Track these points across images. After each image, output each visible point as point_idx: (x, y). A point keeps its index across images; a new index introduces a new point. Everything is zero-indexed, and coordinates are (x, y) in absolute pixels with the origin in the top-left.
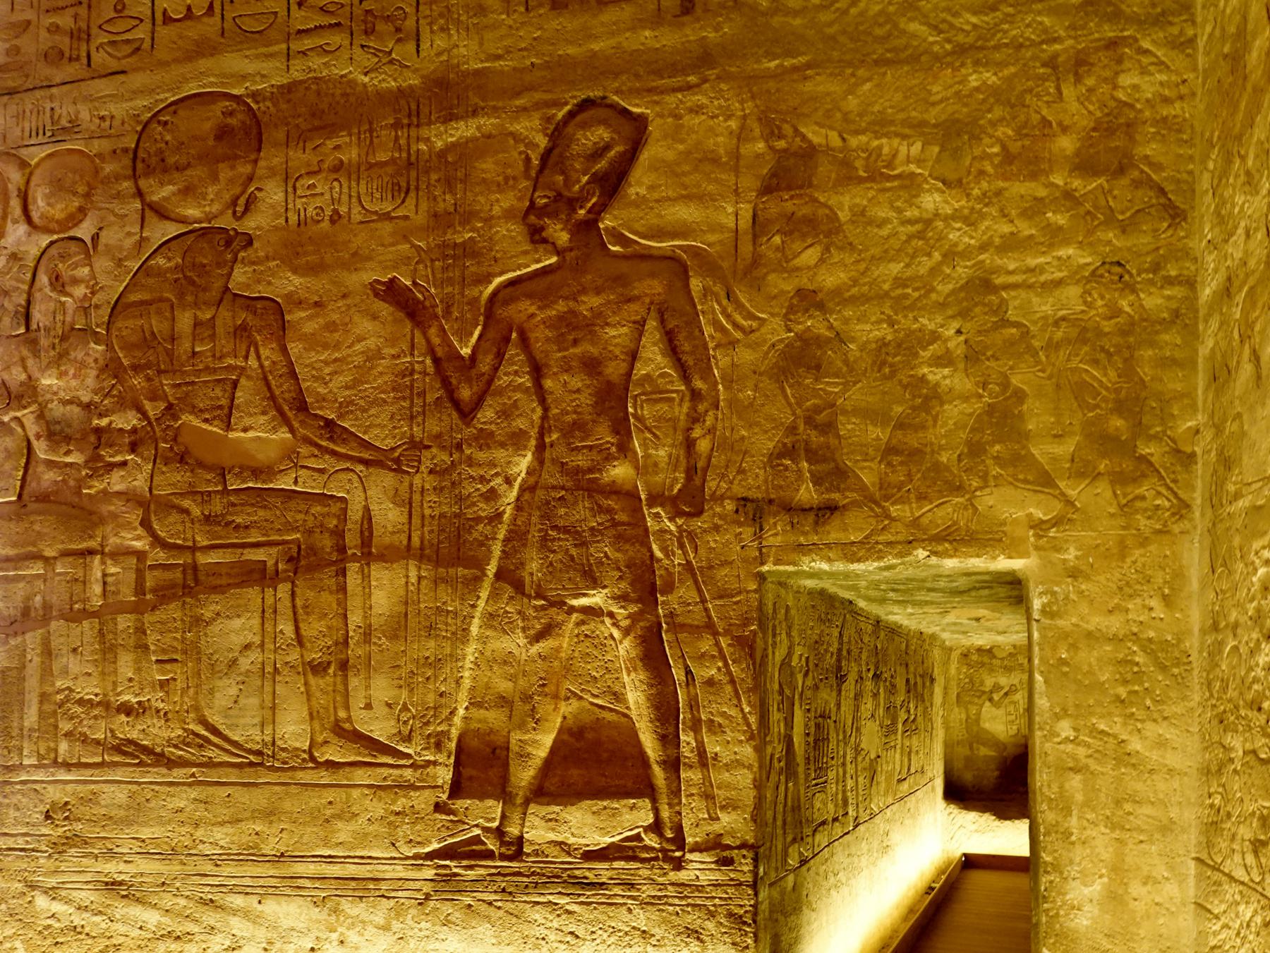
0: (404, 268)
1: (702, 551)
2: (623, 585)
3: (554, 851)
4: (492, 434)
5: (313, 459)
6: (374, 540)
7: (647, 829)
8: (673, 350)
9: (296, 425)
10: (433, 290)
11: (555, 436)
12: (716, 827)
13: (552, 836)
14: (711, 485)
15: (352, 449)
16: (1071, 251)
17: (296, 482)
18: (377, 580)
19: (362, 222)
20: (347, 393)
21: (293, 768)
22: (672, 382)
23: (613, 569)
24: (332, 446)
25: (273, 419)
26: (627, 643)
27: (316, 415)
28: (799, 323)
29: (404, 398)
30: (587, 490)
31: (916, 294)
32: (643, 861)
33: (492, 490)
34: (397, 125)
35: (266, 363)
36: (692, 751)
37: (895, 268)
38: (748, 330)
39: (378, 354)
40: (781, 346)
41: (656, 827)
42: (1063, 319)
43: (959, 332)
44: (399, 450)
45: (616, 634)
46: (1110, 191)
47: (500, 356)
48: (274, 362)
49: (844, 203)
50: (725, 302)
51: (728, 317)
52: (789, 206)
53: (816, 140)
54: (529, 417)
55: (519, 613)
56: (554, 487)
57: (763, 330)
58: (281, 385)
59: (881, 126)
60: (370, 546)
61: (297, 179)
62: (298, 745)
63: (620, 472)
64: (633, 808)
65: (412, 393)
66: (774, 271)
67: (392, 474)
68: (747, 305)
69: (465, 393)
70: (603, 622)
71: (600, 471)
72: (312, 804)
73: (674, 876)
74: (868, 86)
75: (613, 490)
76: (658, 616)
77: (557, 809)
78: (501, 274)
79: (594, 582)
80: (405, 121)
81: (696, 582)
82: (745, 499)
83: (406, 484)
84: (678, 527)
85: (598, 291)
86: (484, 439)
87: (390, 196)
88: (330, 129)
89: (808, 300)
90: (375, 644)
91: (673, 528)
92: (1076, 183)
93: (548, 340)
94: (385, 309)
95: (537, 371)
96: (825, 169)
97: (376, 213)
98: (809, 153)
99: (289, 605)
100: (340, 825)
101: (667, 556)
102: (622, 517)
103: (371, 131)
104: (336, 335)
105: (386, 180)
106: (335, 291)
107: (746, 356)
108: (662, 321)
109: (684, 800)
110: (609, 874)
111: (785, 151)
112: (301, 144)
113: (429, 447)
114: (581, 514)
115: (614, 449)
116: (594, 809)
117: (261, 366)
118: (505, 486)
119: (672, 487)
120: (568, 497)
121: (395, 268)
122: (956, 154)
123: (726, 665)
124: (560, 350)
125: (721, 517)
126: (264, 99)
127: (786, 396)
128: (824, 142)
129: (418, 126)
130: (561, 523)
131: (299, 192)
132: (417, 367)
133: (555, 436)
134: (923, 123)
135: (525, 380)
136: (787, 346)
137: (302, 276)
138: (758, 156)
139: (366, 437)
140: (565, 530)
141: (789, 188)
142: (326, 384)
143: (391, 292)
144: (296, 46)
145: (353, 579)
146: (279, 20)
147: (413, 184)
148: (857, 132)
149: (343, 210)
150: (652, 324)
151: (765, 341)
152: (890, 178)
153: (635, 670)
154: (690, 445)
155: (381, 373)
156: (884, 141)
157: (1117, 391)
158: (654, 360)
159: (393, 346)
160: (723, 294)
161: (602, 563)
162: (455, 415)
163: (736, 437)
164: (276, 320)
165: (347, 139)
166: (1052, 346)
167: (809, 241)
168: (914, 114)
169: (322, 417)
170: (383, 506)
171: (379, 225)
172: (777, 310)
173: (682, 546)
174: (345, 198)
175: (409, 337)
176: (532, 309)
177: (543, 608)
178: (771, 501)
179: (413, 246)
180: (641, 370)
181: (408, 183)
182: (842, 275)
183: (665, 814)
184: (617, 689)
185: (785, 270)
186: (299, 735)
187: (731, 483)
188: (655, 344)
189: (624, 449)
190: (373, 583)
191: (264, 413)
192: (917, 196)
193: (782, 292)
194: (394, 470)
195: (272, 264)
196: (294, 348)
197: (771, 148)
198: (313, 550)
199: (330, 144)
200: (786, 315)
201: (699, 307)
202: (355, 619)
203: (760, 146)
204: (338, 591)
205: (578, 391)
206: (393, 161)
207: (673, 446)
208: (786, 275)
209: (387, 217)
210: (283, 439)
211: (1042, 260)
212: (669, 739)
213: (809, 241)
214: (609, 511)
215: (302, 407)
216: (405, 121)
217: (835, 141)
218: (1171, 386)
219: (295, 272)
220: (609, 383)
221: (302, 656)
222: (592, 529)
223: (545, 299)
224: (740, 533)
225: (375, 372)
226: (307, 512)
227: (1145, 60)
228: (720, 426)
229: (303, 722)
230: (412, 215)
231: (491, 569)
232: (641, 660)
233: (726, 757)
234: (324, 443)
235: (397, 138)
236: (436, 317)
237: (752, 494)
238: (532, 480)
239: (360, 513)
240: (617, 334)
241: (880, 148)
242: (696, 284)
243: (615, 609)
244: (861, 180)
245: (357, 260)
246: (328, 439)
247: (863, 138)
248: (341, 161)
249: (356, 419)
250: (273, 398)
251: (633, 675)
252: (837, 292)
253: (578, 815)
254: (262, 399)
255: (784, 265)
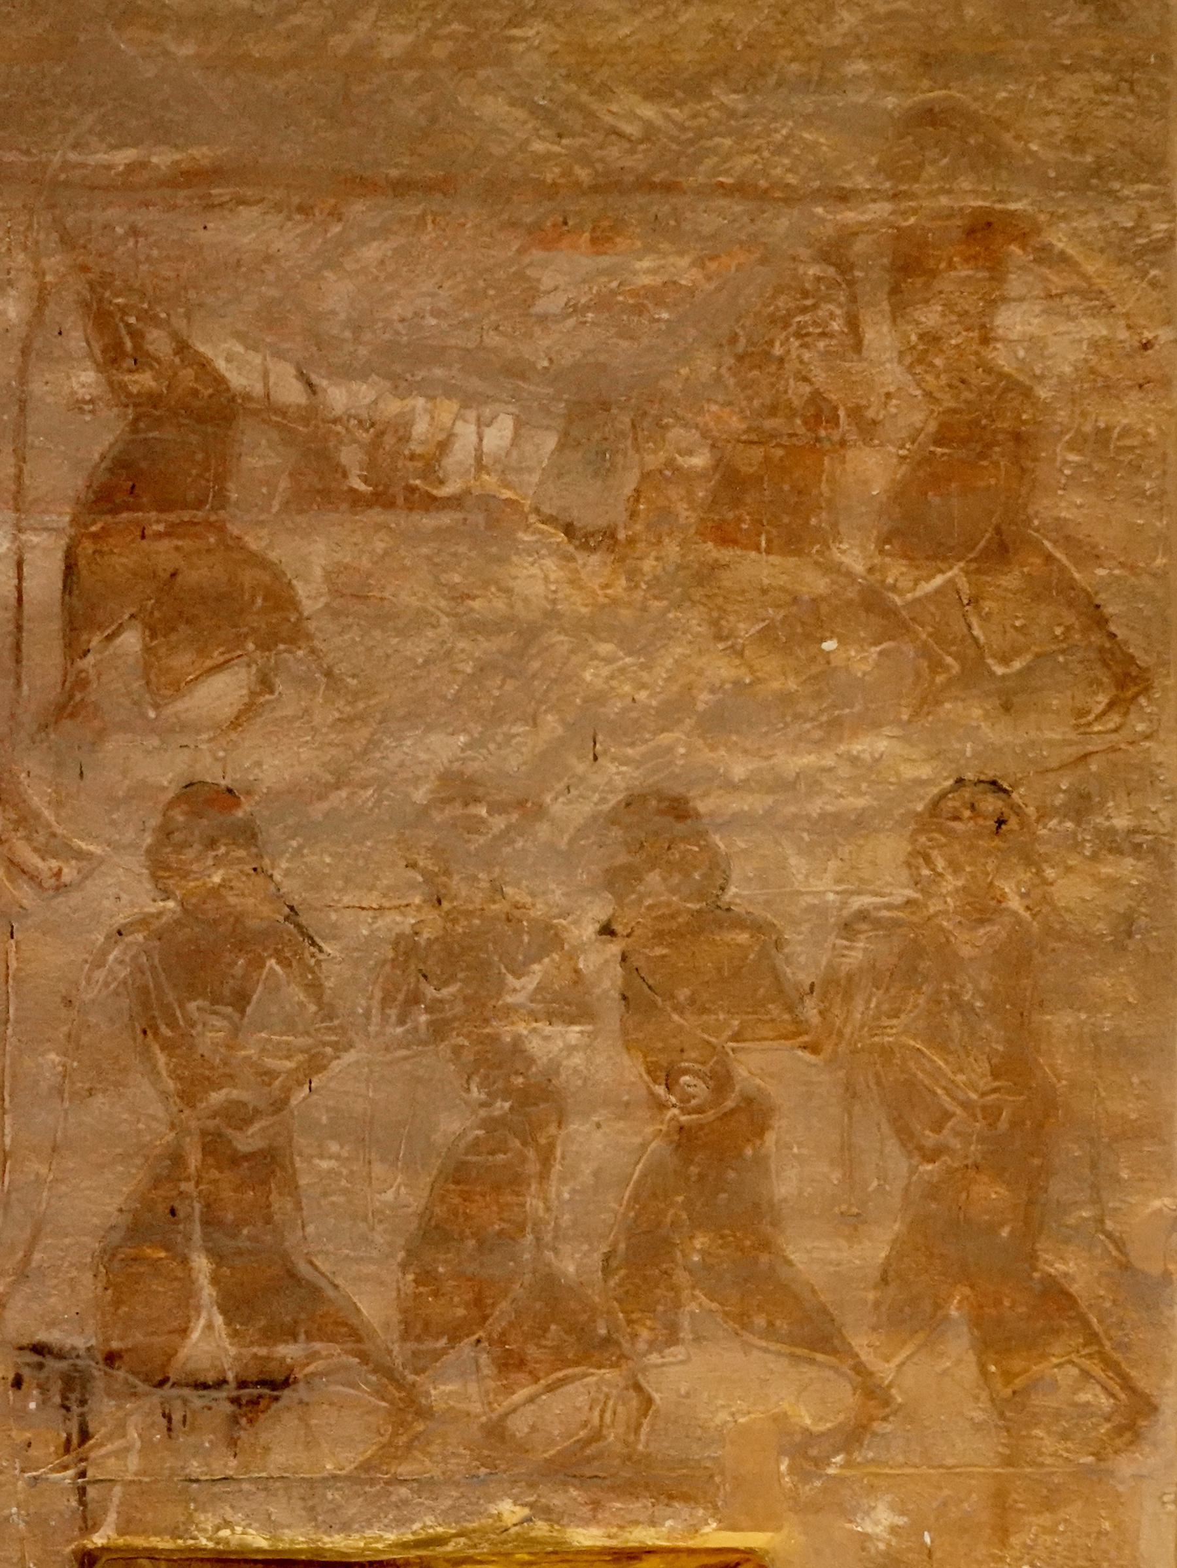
16: (882, 745)
31: (499, 823)
37: (443, 748)
42: (863, 915)
43: (607, 930)
46: (974, 601)
49: (311, 557)
53: (237, 380)
92: (896, 571)
96: (260, 457)
111: (154, 399)
122: (602, 465)
128: (258, 389)
134: (517, 370)
138: (78, 405)
148: (347, 373)
152: (432, 503)
157: (991, 1114)
166: (837, 986)
167: (217, 657)
168: (493, 340)
182: (305, 753)
192: (502, 560)
197: (117, 388)
203: (86, 379)
211: (809, 760)
213: (217, 657)
217: (291, 393)
218: (1114, 1106)
227: (1058, 281)
244: (356, 501)
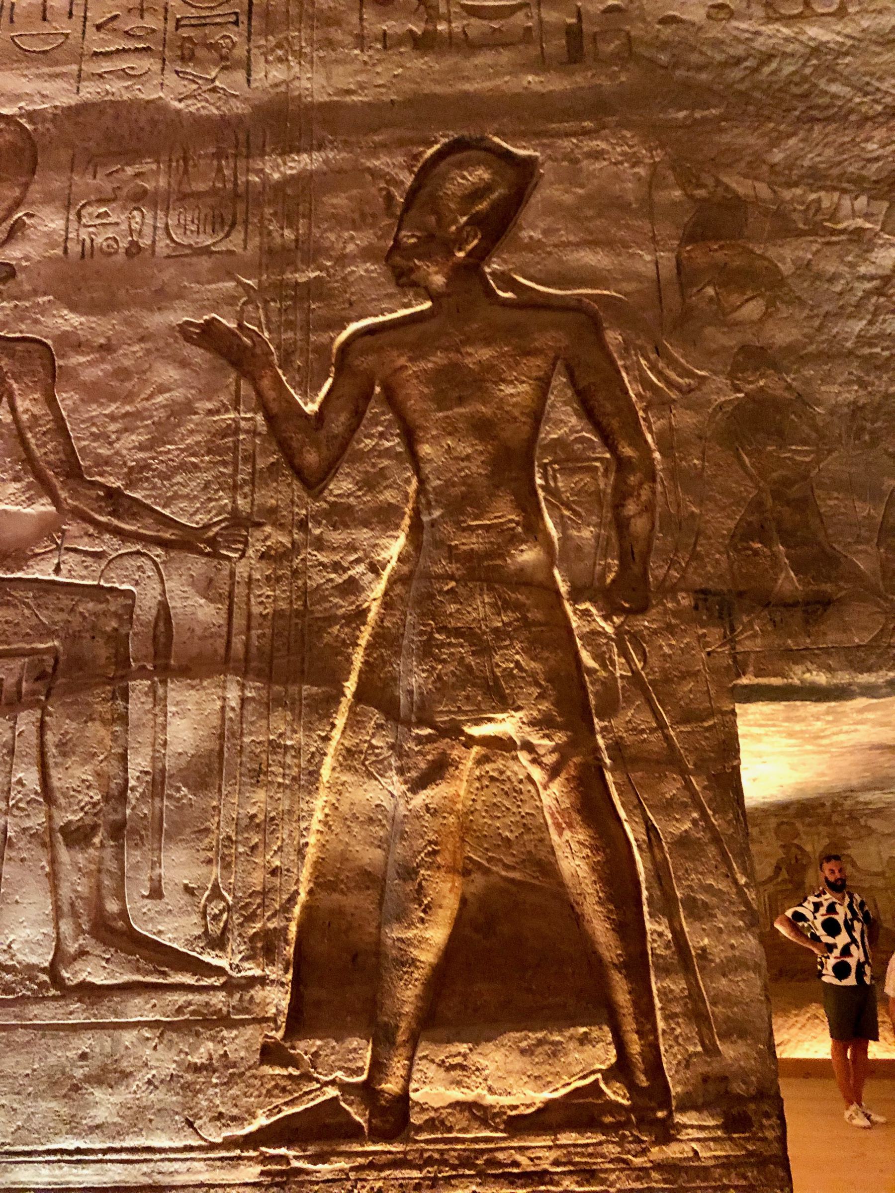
0: (227, 308)
1: (654, 661)
2: (544, 706)
3: (459, 1120)
4: (350, 507)
5: (86, 539)
6: (174, 648)
7: (609, 1075)
8: (589, 412)
9: (63, 494)
10: (266, 335)
11: (437, 513)
12: (716, 1067)
13: (457, 1094)
14: (657, 570)
15: (145, 527)
17: (57, 570)
18: (177, 704)
19: (169, 257)
20: (141, 455)
21: (22, 1000)
22: (594, 449)
23: (529, 684)
24: (116, 522)
25: (29, 487)
26: (556, 787)
27: (94, 484)
28: (750, 383)
29: (224, 464)
30: (487, 580)
32: (605, 1129)
33: (352, 580)
34: (219, 155)
35: (25, 417)
36: (667, 947)
38: (685, 389)
39: (188, 408)
40: (729, 409)
41: (621, 1070)
44: (216, 529)
45: (538, 774)
47: (358, 414)
48: (34, 416)
50: (653, 356)
51: (660, 374)
52: (720, 256)
54: (400, 490)
55: (392, 747)
56: (438, 577)
57: (705, 389)
58: (44, 445)
59: (816, 178)
60: (168, 657)
61: (84, 206)
62: (33, 960)
63: (528, 555)
64: (584, 1040)
65: (236, 458)
66: (710, 324)
67: (204, 560)
68: (682, 361)
69: (311, 458)
70: (515, 758)
71: (502, 556)
72: (52, 1060)
73: (656, 1153)
74: (792, 141)
75: (523, 580)
76: (597, 749)
77: (463, 1048)
78: (359, 318)
79: (505, 703)
80: (231, 151)
81: (649, 701)
82: (704, 592)
83: (226, 572)
84: (617, 628)
85: (488, 342)
86: (340, 515)
87: (209, 229)
88: (132, 155)
89: (755, 357)
90: (170, 797)
91: (609, 630)
93: (423, 396)
94: (197, 355)
95: (410, 437)
97: (190, 246)
98: (736, 204)
99: (34, 740)
100: (99, 1094)
101: (604, 666)
102: (535, 615)
103: (185, 160)
104: (128, 385)
105: (204, 211)
106: (129, 332)
107: (685, 419)
108: (573, 381)
109: (661, 1025)
110: (553, 1155)
112: (91, 169)
113: (259, 525)
114: (479, 610)
115: (520, 529)
116: (524, 1044)
117: (16, 420)
118: (371, 576)
119: (603, 576)
120: (461, 590)
121: (214, 309)
123: (704, 816)
124: (440, 410)
125: (675, 614)
126: (44, 120)
127: (743, 465)
128: (752, 193)
129: (247, 157)
130: (453, 623)
131: (84, 221)
132: (243, 424)
133: (437, 513)
135: (393, 443)
136: (735, 408)
137: (82, 314)
139: (167, 512)
140: (457, 632)
141: (717, 238)
142: (111, 444)
143: (208, 335)
144: (90, 67)
145: (138, 704)
146: (71, 41)
147: (240, 218)
148: (790, 185)
149: (145, 242)
150: (560, 380)
151: (709, 402)
152: (833, 232)
153: (570, 826)
154: (621, 525)
155: (192, 432)
156: (822, 194)
158: (565, 422)
159: (209, 399)
160: (649, 347)
161: (513, 677)
162: (296, 485)
163: (684, 513)
164: (43, 366)
165: (154, 167)
167: (749, 294)
169: (102, 486)
170: (190, 602)
171: (194, 260)
172: (720, 367)
173: (624, 653)
174: (148, 230)
175: (233, 388)
176: (403, 361)
177: (429, 739)
178: (741, 594)
179: (239, 283)
180: (550, 433)
181: (234, 216)
182: (794, 331)
183: (635, 1047)
184: (542, 854)
185: (724, 324)
186: (38, 943)
187: (684, 570)
188: (565, 403)
189: (533, 529)
190: (171, 709)
191: (16, 479)
193: (724, 348)
194: (208, 555)
195: (41, 300)
196: (66, 399)
198: (77, 663)
199: (130, 171)
200: (732, 371)
201: (620, 363)
202: (139, 763)
204: (114, 721)
205: (468, 458)
206: (214, 192)
207: (598, 525)
208: (726, 329)
209: (206, 251)
210: (42, 516)
212: (630, 929)
213: (749, 294)
214: (517, 606)
215: (72, 471)
216: (231, 151)
219: (73, 308)
220: (507, 449)
221: (50, 818)
222: (496, 630)
223: (418, 350)
224: (704, 635)
225: (183, 430)
226: (72, 610)
228: (660, 499)
229: (44, 923)
230: (239, 250)
231: (350, 686)
232: (579, 812)
233: (719, 953)
234: (103, 519)
235: (220, 169)
236: (271, 365)
237: (711, 585)
238: (405, 569)
239: (154, 612)
240: (516, 391)
241: (819, 201)
242: (613, 337)
243: (535, 739)
244: (801, 234)
245: (162, 297)
246: (110, 514)
247: (798, 191)
248: (145, 191)
249: (154, 487)
250: (30, 460)
251: (567, 834)
252: (790, 349)
253: (498, 1056)
254: (14, 462)
255: (721, 317)
